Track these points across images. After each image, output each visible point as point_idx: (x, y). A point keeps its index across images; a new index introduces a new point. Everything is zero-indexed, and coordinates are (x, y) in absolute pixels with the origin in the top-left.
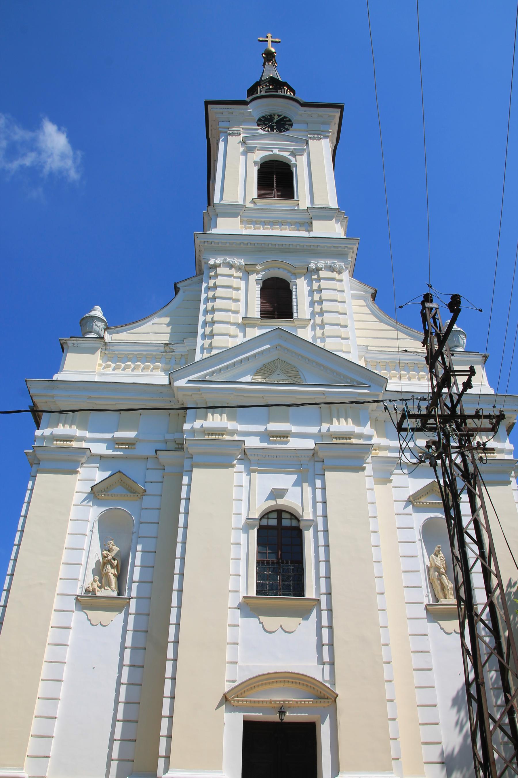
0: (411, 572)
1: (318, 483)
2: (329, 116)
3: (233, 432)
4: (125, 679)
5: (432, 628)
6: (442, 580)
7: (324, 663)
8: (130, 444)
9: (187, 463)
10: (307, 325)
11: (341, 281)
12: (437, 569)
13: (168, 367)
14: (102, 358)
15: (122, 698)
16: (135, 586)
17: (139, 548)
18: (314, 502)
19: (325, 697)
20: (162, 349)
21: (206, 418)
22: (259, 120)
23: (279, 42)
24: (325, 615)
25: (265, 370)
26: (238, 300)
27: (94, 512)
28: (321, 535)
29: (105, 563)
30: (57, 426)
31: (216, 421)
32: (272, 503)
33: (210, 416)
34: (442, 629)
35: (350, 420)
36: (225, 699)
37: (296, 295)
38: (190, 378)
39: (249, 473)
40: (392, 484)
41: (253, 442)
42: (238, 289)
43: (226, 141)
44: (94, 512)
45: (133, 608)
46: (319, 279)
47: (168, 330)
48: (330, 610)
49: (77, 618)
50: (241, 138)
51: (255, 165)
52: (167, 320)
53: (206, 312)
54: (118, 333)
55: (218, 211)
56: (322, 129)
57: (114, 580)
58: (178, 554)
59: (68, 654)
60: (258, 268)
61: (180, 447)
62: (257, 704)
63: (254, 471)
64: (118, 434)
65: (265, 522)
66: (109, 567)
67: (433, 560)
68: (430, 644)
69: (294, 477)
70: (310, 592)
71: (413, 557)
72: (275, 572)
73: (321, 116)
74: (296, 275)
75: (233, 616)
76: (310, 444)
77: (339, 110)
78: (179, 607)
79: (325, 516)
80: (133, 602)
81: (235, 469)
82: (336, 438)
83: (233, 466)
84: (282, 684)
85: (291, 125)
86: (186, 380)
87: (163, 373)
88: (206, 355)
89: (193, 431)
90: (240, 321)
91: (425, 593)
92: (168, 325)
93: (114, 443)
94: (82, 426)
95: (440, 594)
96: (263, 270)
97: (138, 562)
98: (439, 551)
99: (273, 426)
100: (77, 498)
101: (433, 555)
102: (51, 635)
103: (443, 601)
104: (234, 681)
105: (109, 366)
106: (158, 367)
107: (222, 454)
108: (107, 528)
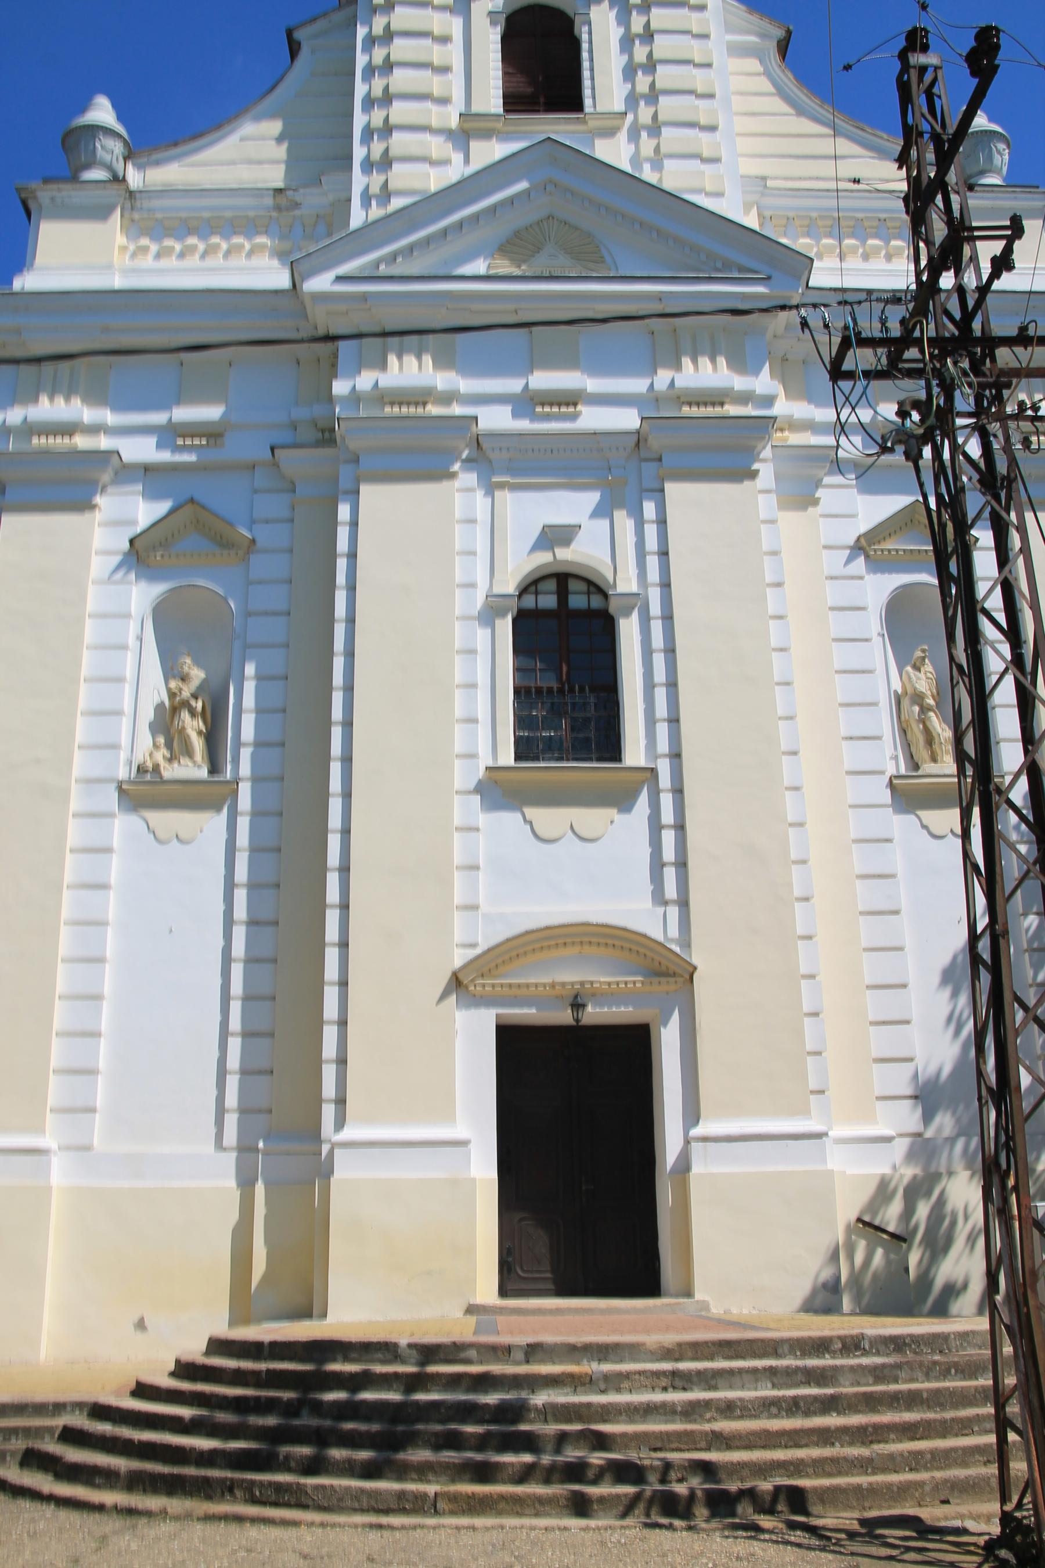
0: (859, 705)
1: (649, 509)
3: (449, 397)
6: (928, 724)
7: (666, 903)
8: (213, 434)
9: (345, 473)
12: (918, 698)
13: (287, 245)
14: (125, 229)
16: (246, 754)
17: (250, 669)
19: (670, 973)
20: (269, 201)
21: (383, 366)
24: (667, 800)
25: (519, 245)
26: (445, 70)
27: (141, 596)
28: (657, 628)
30: (36, 400)
31: (407, 370)
32: (544, 558)
33: (392, 359)
34: (924, 827)
35: (722, 361)
36: (457, 983)
37: (591, 51)
38: (343, 269)
39: (490, 489)
40: (819, 509)
41: (496, 419)
42: (445, 40)
44: (141, 596)
47: (281, 152)
48: (678, 791)
49: (124, 827)
52: (276, 127)
53: (369, 103)
54: (158, 163)
57: (198, 744)
59: (112, 906)
61: (326, 436)
62: (524, 991)
63: (501, 486)
64: (183, 414)
65: (529, 601)
66: (185, 715)
67: (910, 678)
68: (896, 859)
70: (634, 752)
71: (863, 672)
72: (557, 712)
75: (467, 808)
76: (628, 419)
79: (666, 585)
80: (245, 791)
81: (457, 484)
83: (453, 476)
84: (576, 949)
86: (330, 275)
87: (275, 263)
88: (376, 212)
89: (355, 397)
90: (454, 122)
91: (889, 751)
92: (280, 140)
93: (171, 434)
95: (922, 752)
97: (249, 700)
98: (923, 658)
99: (543, 380)
100: (100, 566)
101: (909, 668)
102: (72, 868)
103: (928, 767)
104: (473, 946)
105: (145, 250)
106: (262, 247)
107: (427, 449)
108: (176, 630)
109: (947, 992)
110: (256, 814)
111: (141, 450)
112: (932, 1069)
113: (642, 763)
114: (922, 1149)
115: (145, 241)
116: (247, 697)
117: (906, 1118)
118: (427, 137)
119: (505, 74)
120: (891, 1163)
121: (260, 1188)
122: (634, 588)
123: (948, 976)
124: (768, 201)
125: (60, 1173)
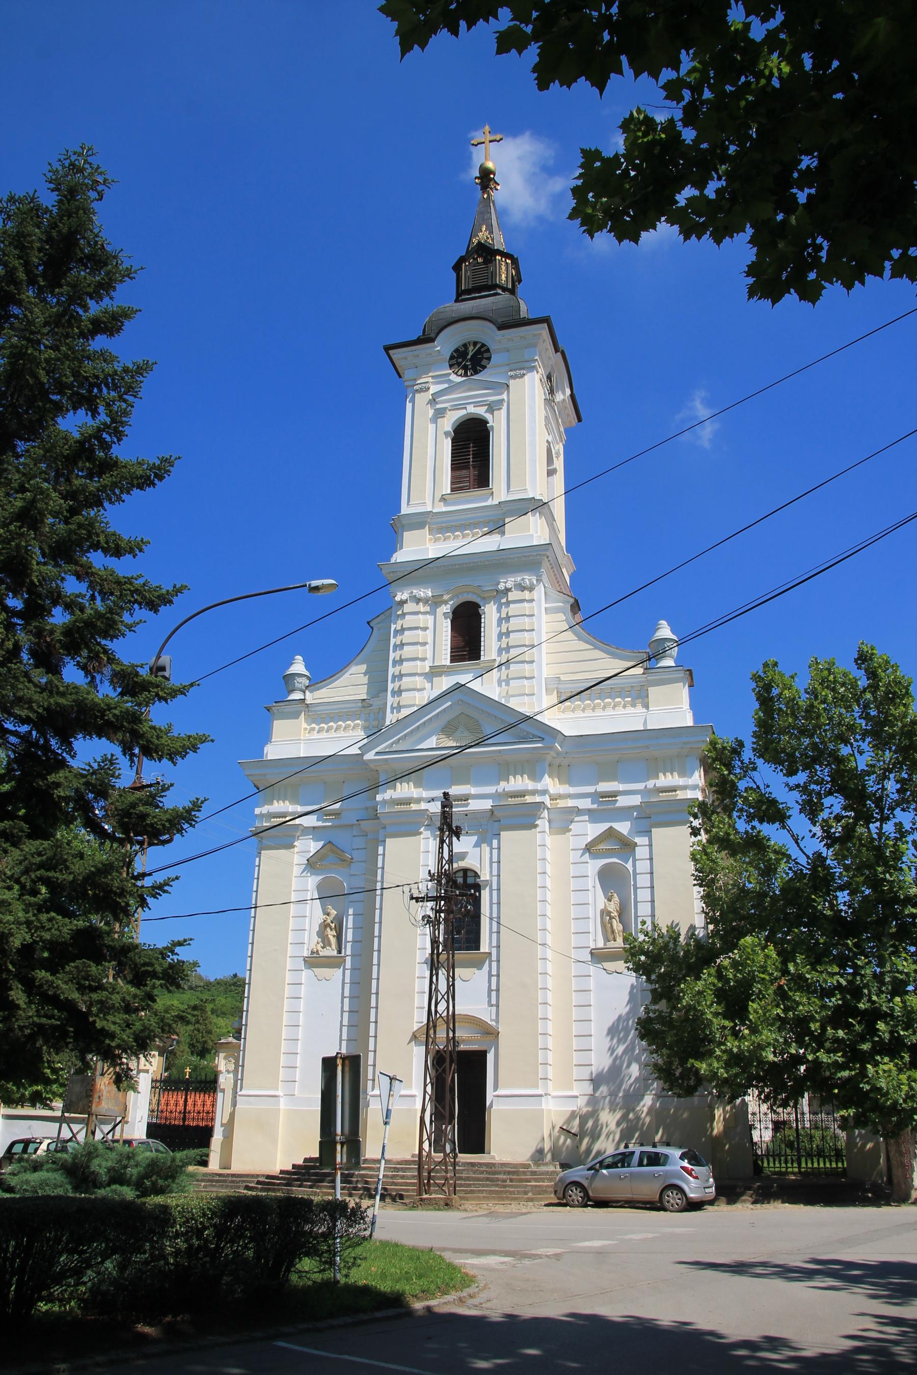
1: (495, 842)
2: (534, 335)
3: (418, 801)
4: (345, 1022)
5: (592, 969)
7: (492, 1006)
8: (337, 814)
11: (532, 601)
12: (609, 913)
13: (367, 724)
15: (345, 1037)
17: (351, 911)
18: (491, 862)
19: (491, 1033)
20: (360, 705)
21: (395, 788)
22: (452, 357)
23: (501, 139)
24: (494, 964)
25: (448, 729)
26: (425, 644)
27: (312, 881)
28: (495, 893)
29: (324, 926)
30: (272, 804)
31: (405, 790)
33: (398, 785)
35: (525, 776)
38: (377, 750)
40: (571, 833)
42: (425, 629)
43: (413, 401)
44: (312, 881)
45: (348, 964)
46: (508, 603)
47: (365, 680)
50: (428, 396)
51: (446, 438)
52: (363, 668)
53: (395, 663)
55: (404, 522)
56: (526, 358)
57: (333, 941)
60: (446, 597)
61: (376, 817)
66: (328, 929)
69: (475, 838)
70: (484, 947)
74: (487, 600)
76: (487, 804)
77: (545, 325)
78: (379, 965)
80: (348, 959)
81: (422, 836)
82: (511, 797)
83: (420, 833)
85: (489, 359)
89: (384, 802)
90: (427, 670)
92: (365, 674)
94: (295, 800)
97: (350, 925)
100: (297, 870)
105: (313, 729)
106: (358, 725)
109: (609, 1038)
110: (353, 969)
112: (600, 1069)
114: (593, 1100)
115: (313, 725)
117: (588, 1088)
118: (417, 678)
119: (452, 637)
120: (581, 1105)
122: (488, 878)
123: (612, 1031)
124: (560, 686)
125: (283, 1104)
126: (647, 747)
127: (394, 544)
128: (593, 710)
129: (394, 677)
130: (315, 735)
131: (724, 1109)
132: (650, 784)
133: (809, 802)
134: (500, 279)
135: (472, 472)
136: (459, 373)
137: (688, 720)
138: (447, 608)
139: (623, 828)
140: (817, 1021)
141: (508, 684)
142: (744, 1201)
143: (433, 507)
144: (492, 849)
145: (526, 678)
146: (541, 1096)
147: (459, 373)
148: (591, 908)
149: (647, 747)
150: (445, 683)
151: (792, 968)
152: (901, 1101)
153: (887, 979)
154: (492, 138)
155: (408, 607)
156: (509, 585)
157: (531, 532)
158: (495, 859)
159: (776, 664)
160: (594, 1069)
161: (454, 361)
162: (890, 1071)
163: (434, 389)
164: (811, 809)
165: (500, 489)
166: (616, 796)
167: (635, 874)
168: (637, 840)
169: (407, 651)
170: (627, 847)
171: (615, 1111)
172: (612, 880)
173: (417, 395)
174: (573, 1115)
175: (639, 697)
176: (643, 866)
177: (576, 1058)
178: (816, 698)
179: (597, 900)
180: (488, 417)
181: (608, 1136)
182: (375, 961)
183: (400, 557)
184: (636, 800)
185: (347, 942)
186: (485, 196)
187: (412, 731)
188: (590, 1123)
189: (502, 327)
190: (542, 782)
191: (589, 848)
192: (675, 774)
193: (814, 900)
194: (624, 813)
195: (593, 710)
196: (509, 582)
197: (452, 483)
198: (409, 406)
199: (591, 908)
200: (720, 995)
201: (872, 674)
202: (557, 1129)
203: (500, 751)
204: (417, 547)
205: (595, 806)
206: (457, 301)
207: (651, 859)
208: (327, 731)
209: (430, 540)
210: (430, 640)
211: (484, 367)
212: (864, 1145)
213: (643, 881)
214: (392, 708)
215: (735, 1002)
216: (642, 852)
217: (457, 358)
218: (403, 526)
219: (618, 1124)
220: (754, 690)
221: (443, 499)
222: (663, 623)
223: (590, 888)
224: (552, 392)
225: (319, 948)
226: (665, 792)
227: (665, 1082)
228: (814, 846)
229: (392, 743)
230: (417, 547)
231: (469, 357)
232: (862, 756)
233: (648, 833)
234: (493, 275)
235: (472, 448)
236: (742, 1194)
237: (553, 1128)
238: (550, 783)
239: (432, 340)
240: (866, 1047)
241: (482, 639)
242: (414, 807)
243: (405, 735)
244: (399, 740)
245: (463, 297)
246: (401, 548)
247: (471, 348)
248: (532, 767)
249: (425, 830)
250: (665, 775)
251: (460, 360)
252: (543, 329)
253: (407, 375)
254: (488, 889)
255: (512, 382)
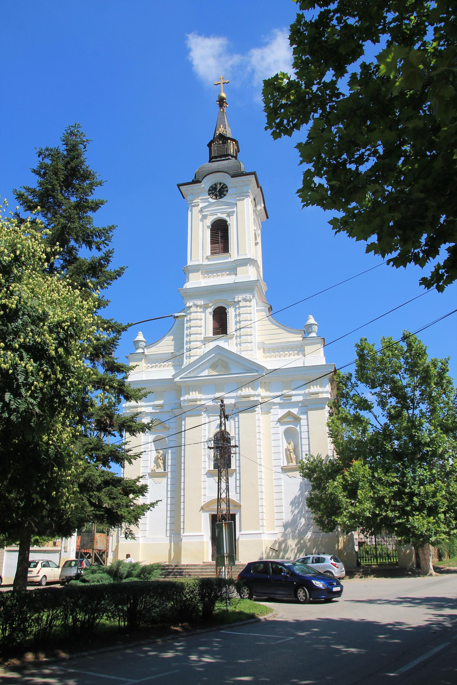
1: (236, 419)
2: (248, 180)
3: (200, 400)
4: (169, 502)
5: (283, 476)
8: (161, 406)
10: (233, 337)
11: (251, 306)
12: (289, 450)
13: (174, 364)
14: (145, 362)
15: (169, 509)
16: (169, 467)
18: (235, 428)
20: (171, 355)
22: (209, 190)
24: (238, 475)
25: (214, 367)
26: (201, 327)
29: (157, 458)
31: (194, 395)
35: (250, 388)
36: (202, 508)
38: (180, 377)
40: (271, 414)
42: (201, 320)
43: (191, 211)
46: (239, 308)
47: (173, 343)
50: (199, 208)
52: (172, 337)
55: (189, 269)
57: (162, 465)
58: (183, 455)
60: (210, 305)
63: (211, 416)
64: (157, 403)
66: (159, 460)
70: (233, 467)
73: (244, 181)
74: (230, 306)
75: (204, 478)
78: (184, 476)
80: (169, 474)
81: (203, 416)
82: (244, 398)
83: (202, 415)
85: (227, 191)
87: (172, 368)
89: (185, 401)
90: (203, 339)
92: (173, 340)
93: (155, 406)
96: (212, 306)
97: (170, 457)
109: (291, 506)
111: (150, 410)
112: (287, 520)
113: (234, 468)
114: (284, 535)
115: (149, 365)
116: (169, 456)
117: (282, 530)
118: (198, 343)
119: (214, 323)
120: (279, 537)
121: (172, 543)
122: (234, 435)
123: (292, 503)
126: (305, 374)
127: (185, 279)
128: (280, 357)
129: (187, 342)
130: (150, 370)
131: (343, 537)
132: (307, 391)
133: (382, 401)
134: (230, 152)
135: (221, 245)
136: (213, 198)
137: (323, 361)
138: (211, 310)
139: (295, 411)
140: (388, 498)
141: (240, 346)
142: (356, 577)
143: (203, 262)
144: (235, 422)
145: (249, 343)
146: (261, 534)
147: (213, 198)
148: (281, 448)
149: (305, 374)
150: (212, 345)
151: (376, 475)
152: (424, 532)
153: (417, 479)
154: (224, 82)
155: (192, 310)
156: (240, 299)
157: (250, 274)
158: (237, 426)
159: (366, 340)
160: (284, 521)
161: (211, 192)
162: (419, 518)
163: (201, 205)
164: (382, 404)
165: (234, 254)
166: (291, 397)
167: (301, 432)
168: (302, 417)
169: (193, 330)
170: (297, 420)
171: (294, 539)
172: (290, 435)
173: (193, 208)
174: (275, 542)
175: (300, 351)
176: (304, 428)
177: (276, 516)
178: (385, 355)
179: (285, 444)
180: (227, 219)
181: (291, 551)
182: (182, 474)
183: (188, 285)
184: (300, 398)
185: (168, 465)
186: (222, 110)
187: (196, 368)
188: (283, 545)
189: (233, 176)
190: (258, 391)
191: (280, 421)
192: (318, 386)
193: (385, 445)
194: (295, 404)
195: (280, 357)
196: (239, 297)
197: (211, 250)
198: (190, 213)
199: (281, 448)
200: (345, 488)
201: (409, 345)
202: (269, 548)
203: (238, 377)
204: (196, 281)
205: (282, 401)
206: (210, 162)
207: (308, 425)
208: (155, 367)
209: (202, 277)
210: (203, 325)
211: (225, 195)
212: (406, 551)
213: (304, 435)
214: (187, 357)
215: (351, 490)
216: (304, 422)
217: (212, 190)
218: (189, 271)
219: (296, 545)
220: (356, 351)
221: (207, 258)
222: (311, 316)
223: (280, 439)
224: (256, 206)
225: (155, 469)
226: (314, 394)
227: (321, 526)
228: (384, 420)
229: (188, 374)
230: (196, 281)
231: (218, 190)
232: (404, 379)
233: (306, 413)
234: (227, 149)
235: (220, 233)
236: (355, 574)
237: (267, 548)
238: (261, 391)
239: (200, 182)
240: (408, 508)
241: (228, 324)
242: (199, 403)
243: (194, 370)
244: (191, 372)
245: (213, 160)
246: (188, 281)
247: (218, 186)
248: (252, 383)
249: (204, 413)
250: (313, 387)
251: (213, 191)
252: (252, 178)
253: (188, 198)
254: (234, 440)
255: (238, 203)
